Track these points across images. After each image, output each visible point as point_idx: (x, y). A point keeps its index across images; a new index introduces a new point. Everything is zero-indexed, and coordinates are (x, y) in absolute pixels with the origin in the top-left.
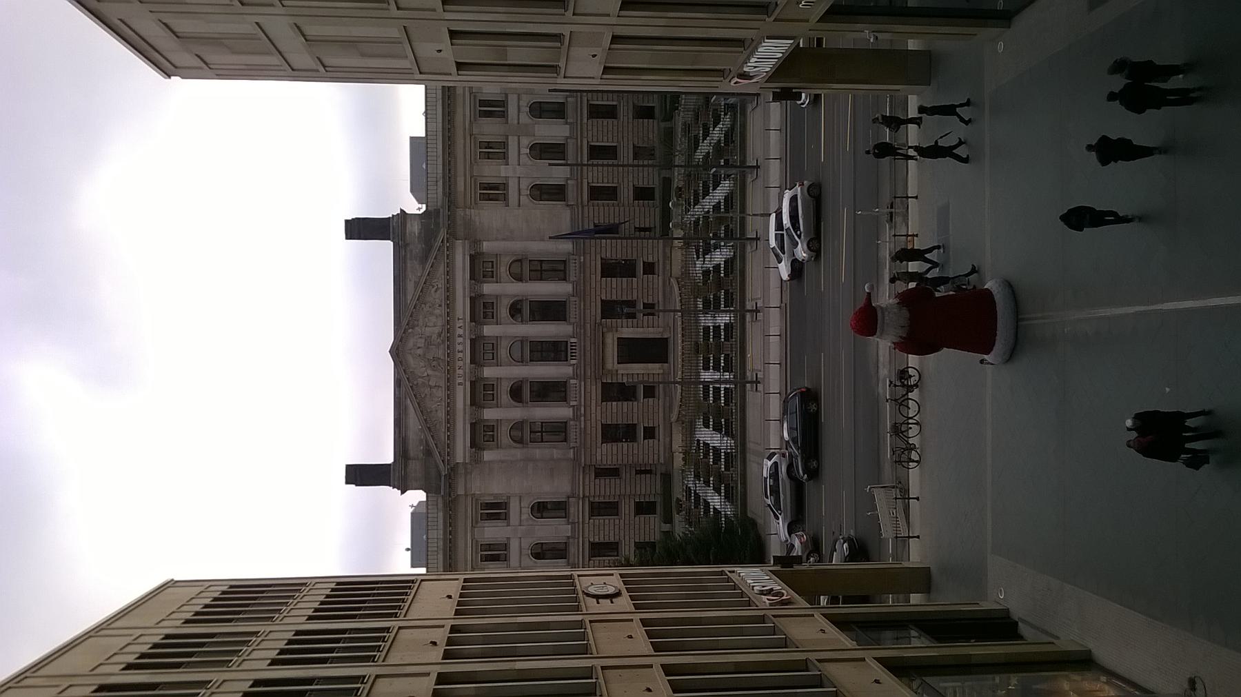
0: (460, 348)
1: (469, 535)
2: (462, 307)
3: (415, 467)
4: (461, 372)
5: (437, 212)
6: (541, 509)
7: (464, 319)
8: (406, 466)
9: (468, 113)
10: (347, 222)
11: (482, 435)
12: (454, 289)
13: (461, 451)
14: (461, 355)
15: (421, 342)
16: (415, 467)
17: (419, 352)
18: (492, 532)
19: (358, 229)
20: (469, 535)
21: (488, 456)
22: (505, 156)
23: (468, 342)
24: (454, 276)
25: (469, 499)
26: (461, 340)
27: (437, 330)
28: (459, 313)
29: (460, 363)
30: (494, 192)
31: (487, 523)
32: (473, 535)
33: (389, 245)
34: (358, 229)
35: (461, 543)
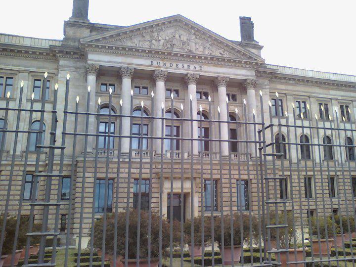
0: (180, 66)
2: (210, 71)
3: (84, 34)
4: (162, 64)
5: (265, 67)
7: (201, 71)
8: (87, 27)
10: (250, 19)
11: (109, 77)
12: (221, 66)
13: (97, 58)
14: (174, 65)
15: (184, 38)
16: (84, 34)
17: (177, 36)
19: (246, 25)
21: (92, 78)
23: (185, 72)
24: (231, 67)
26: (186, 66)
28: (205, 68)
29: (168, 64)
30: (278, 108)
32: (25, 71)
33: (239, 39)
34: (246, 25)
35: (15, 61)
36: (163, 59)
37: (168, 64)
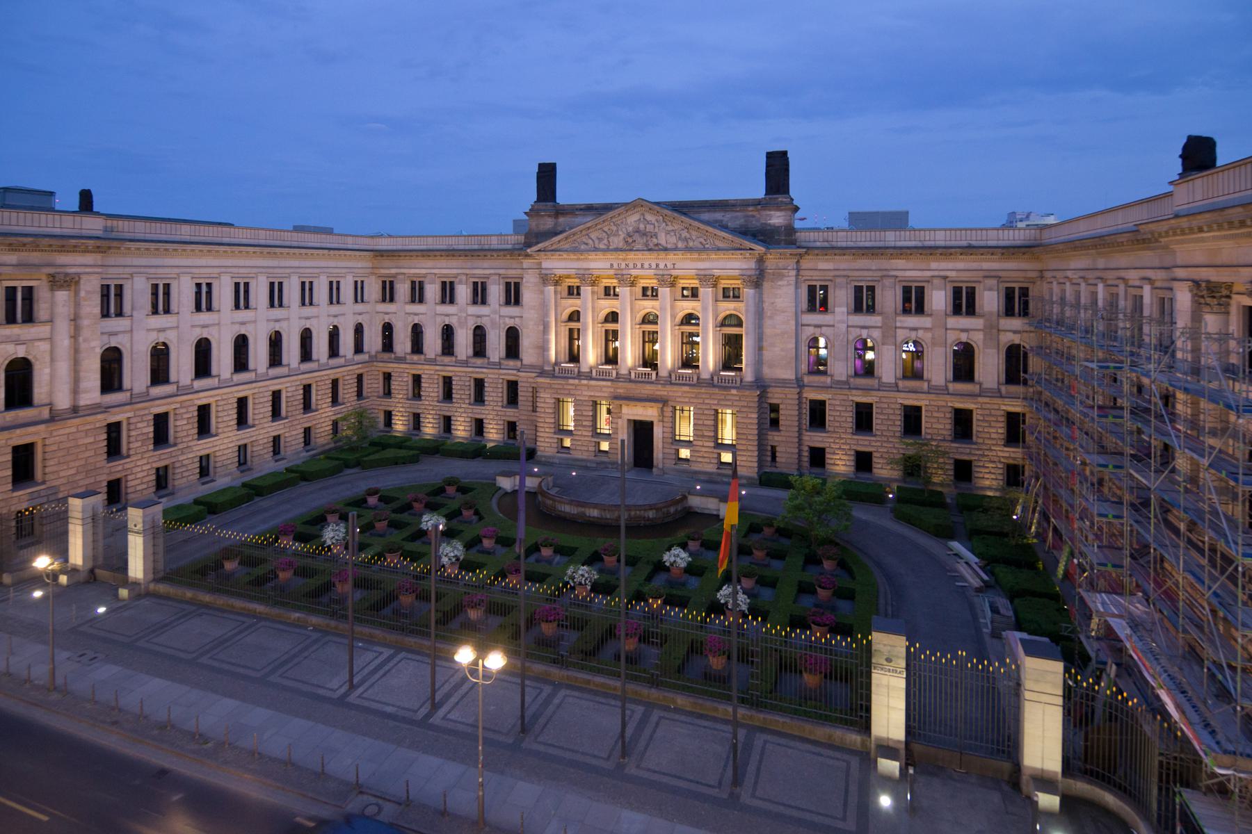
0: (646, 266)
1: (492, 271)
4: (623, 266)
6: (513, 337)
9: (908, 274)
18: (496, 292)
20: (492, 271)
22: (858, 308)
25: (519, 271)
27: (663, 242)
29: (631, 266)
30: (817, 301)
31: (502, 287)
35: (486, 264)
36: (624, 260)
37: (631, 266)
